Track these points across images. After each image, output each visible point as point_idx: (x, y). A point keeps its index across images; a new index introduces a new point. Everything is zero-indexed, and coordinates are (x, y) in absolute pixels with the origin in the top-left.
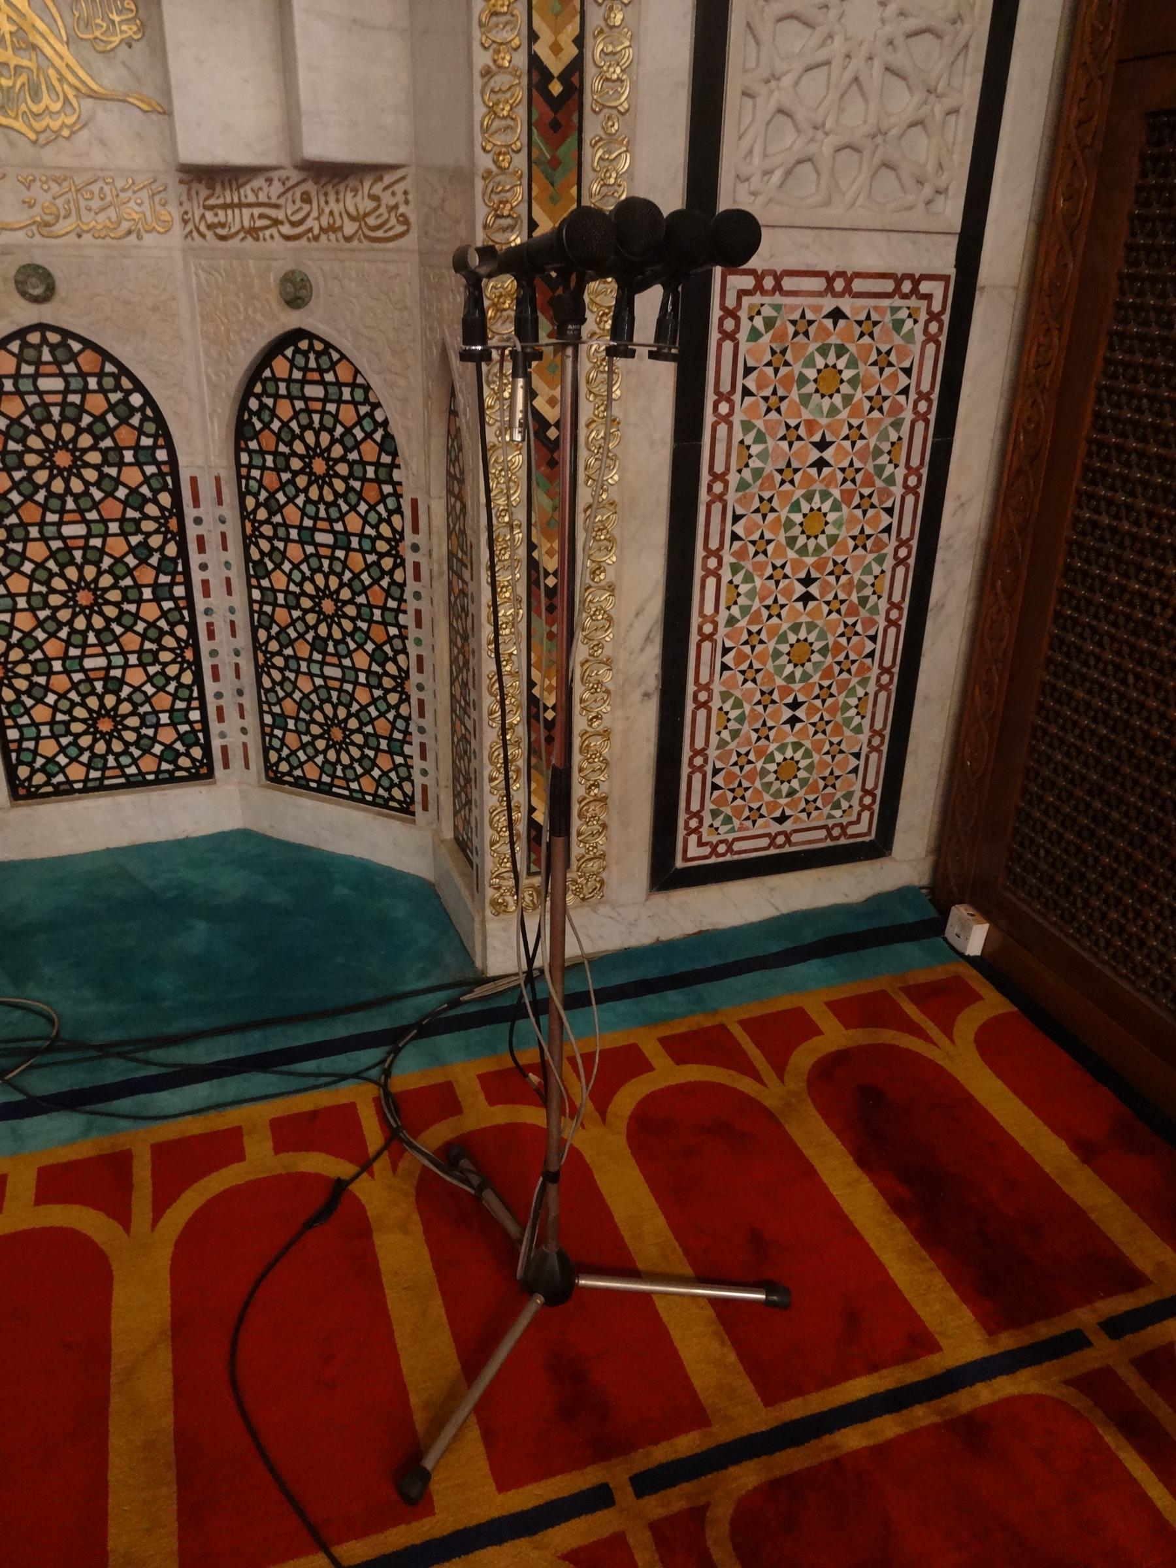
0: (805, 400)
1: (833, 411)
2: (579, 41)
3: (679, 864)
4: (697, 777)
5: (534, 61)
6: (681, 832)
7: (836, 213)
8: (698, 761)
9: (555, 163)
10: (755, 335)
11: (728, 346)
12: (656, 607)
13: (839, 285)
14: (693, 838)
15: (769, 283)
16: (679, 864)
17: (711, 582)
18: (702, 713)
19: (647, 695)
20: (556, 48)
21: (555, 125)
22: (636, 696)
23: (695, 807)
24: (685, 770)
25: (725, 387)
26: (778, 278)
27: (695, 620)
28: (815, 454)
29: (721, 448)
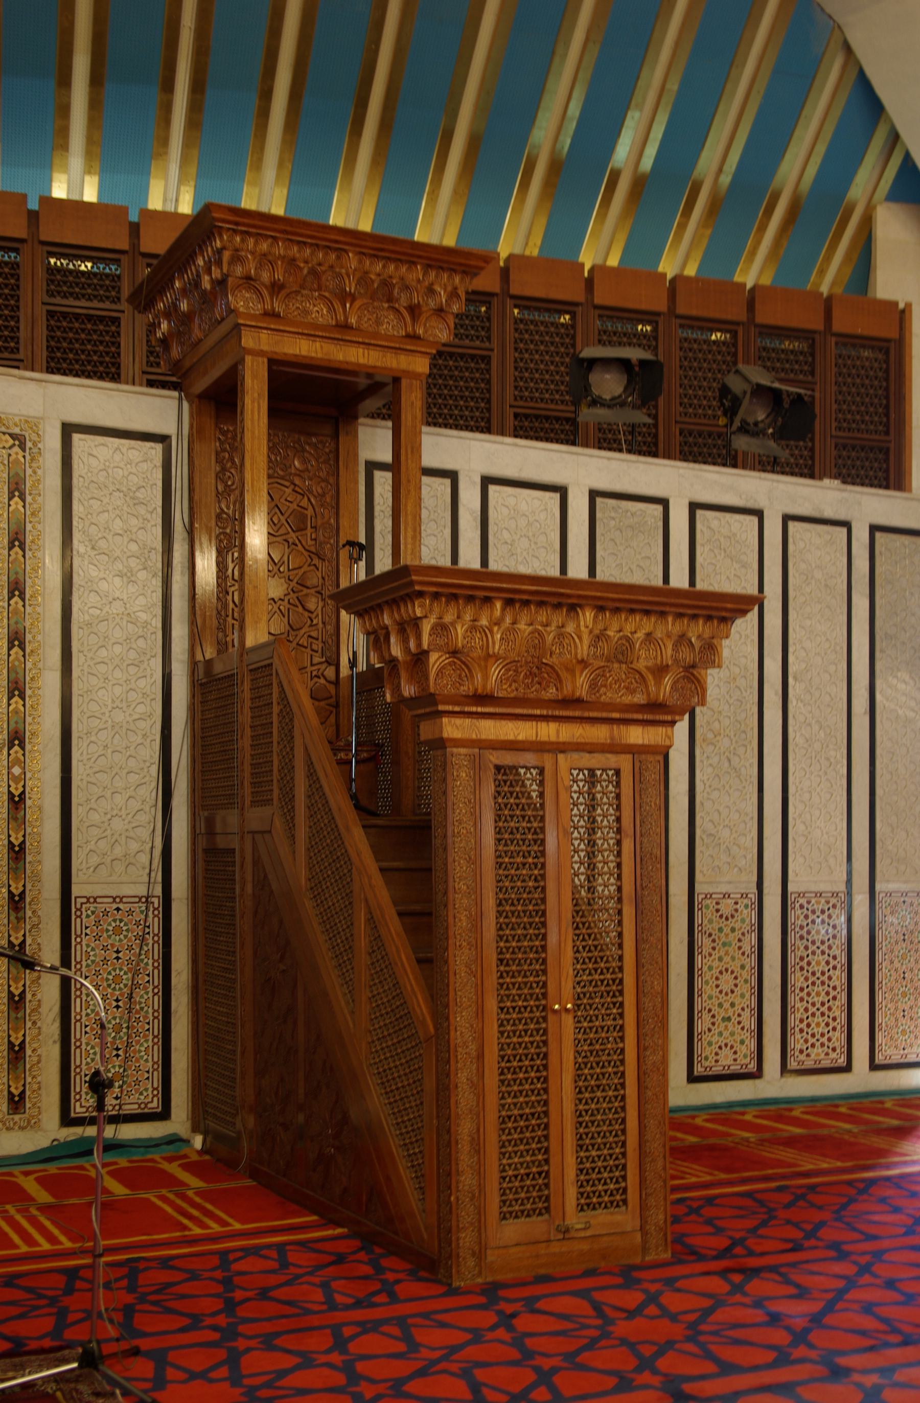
0: (109, 937)
1: (120, 940)
2: (24, 836)
3: (73, 1115)
4: (78, 1077)
5: (10, 842)
6: (73, 1101)
7: (114, 878)
8: (78, 1070)
9: (17, 868)
10: (88, 916)
11: (78, 920)
12: (57, 1008)
13: (118, 900)
14: (78, 1104)
15: (92, 900)
16: (73, 1115)
17: (78, 1000)
18: (78, 1051)
19: (55, 1042)
20: (17, 838)
21: (17, 858)
22: (51, 1042)
23: (78, 1090)
24: (73, 1074)
25: (79, 933)
26: (121, 899)
27: (73, 1015)
28: (115, 955)
29: (78, 953)
